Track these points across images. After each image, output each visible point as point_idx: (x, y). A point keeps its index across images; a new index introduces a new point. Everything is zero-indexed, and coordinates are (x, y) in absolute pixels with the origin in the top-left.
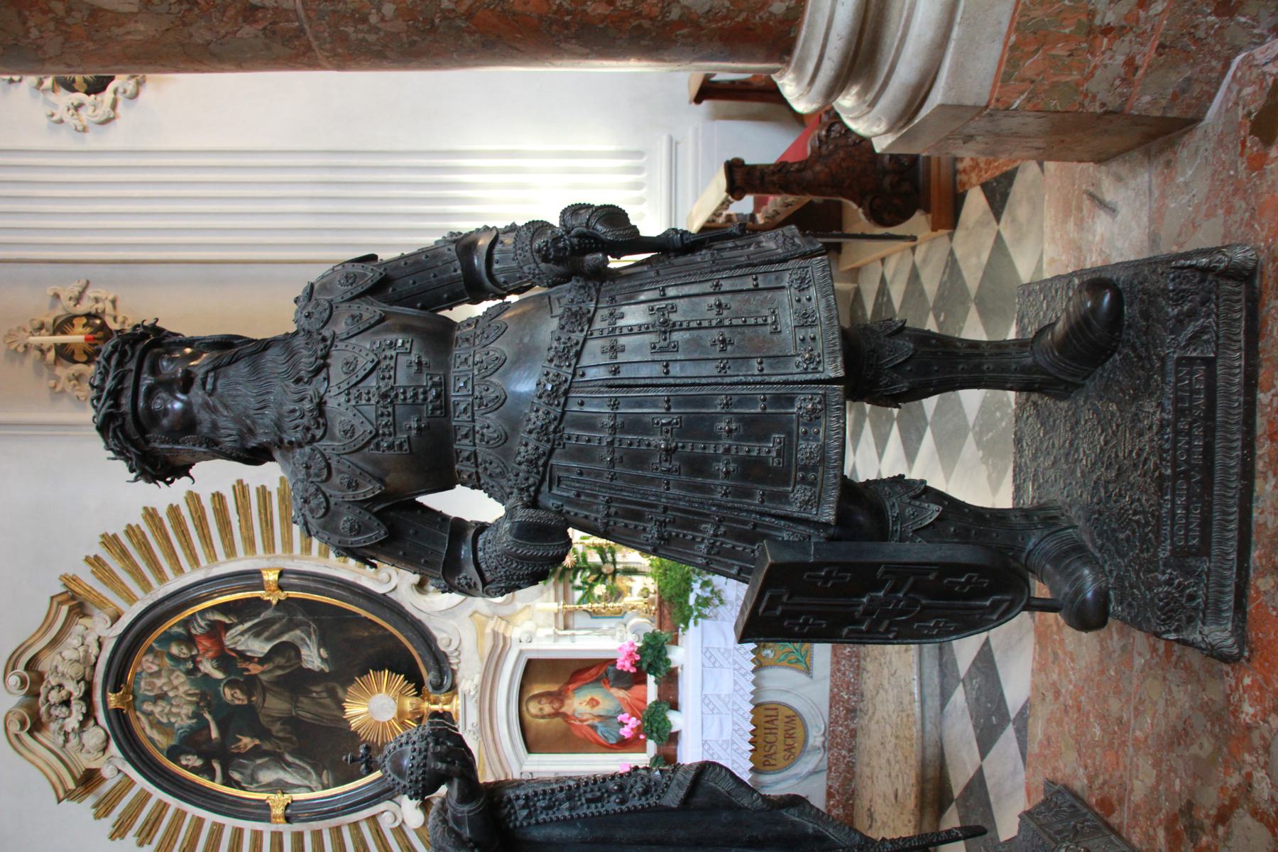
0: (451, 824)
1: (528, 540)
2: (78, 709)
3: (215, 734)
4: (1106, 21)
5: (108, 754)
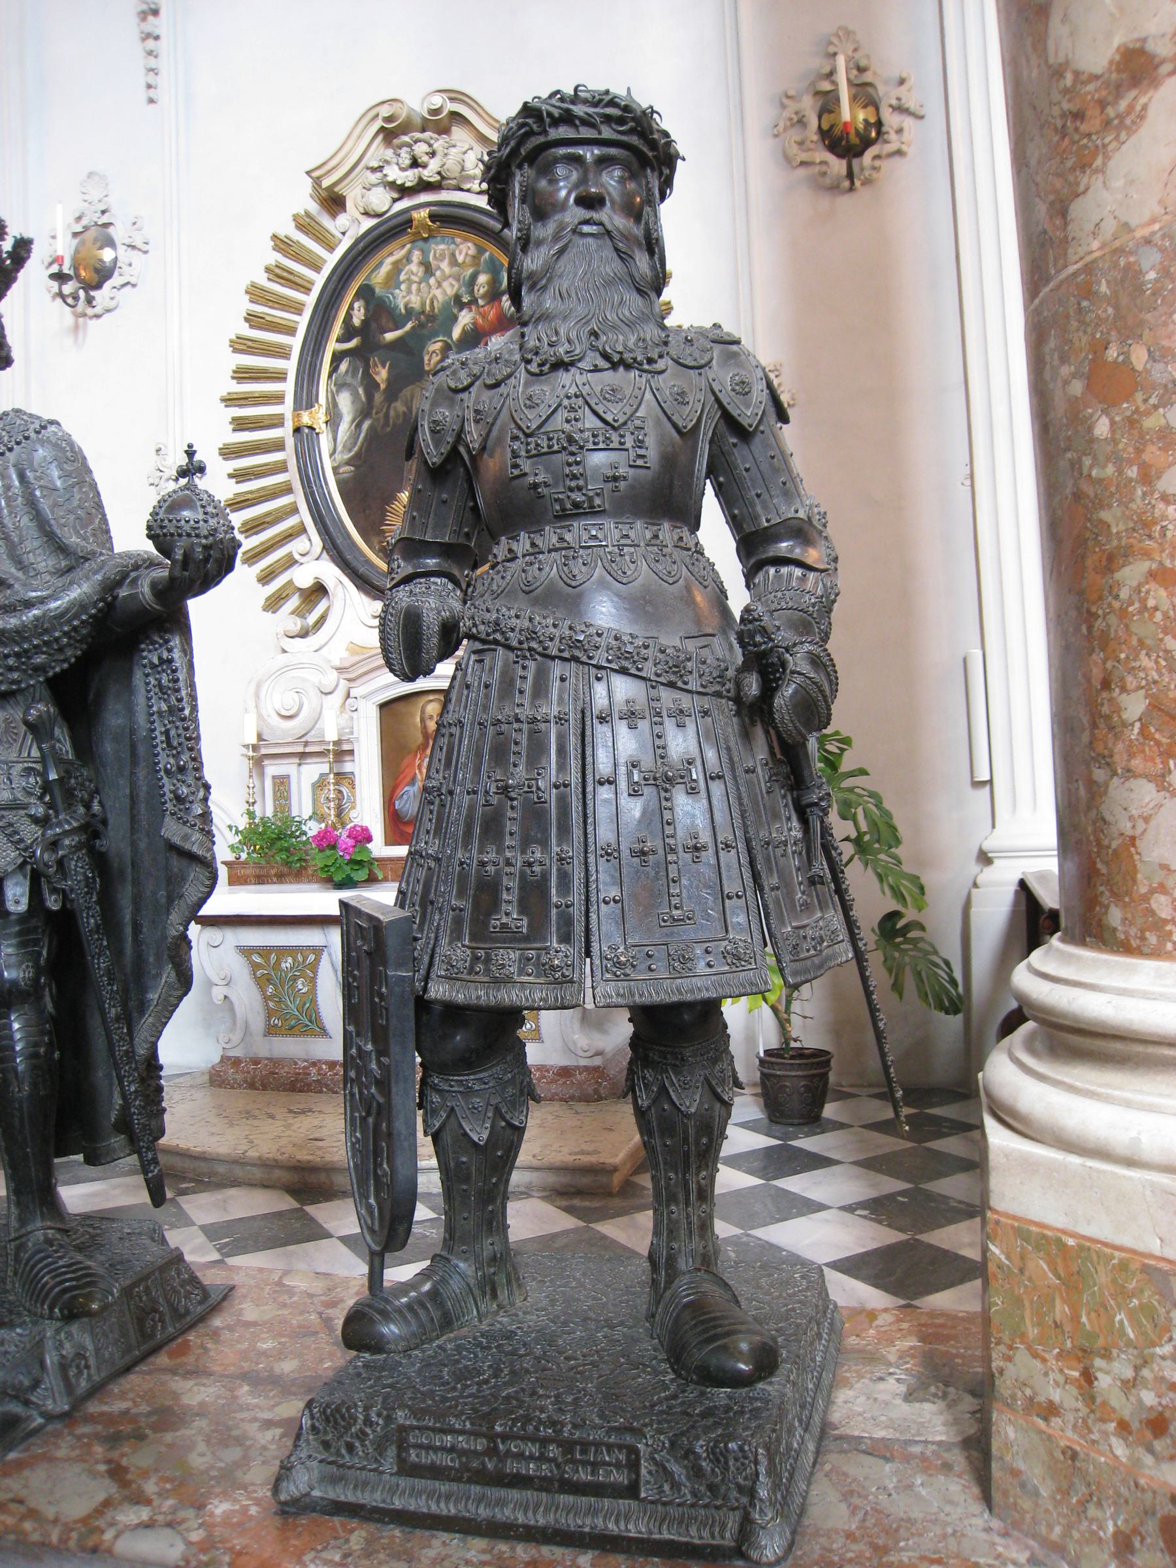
0: (133, 574)
1: (405, 626)
2: (408, 178)
3: (390, 336)
4: (1099, 1375)
5: (362, 218)
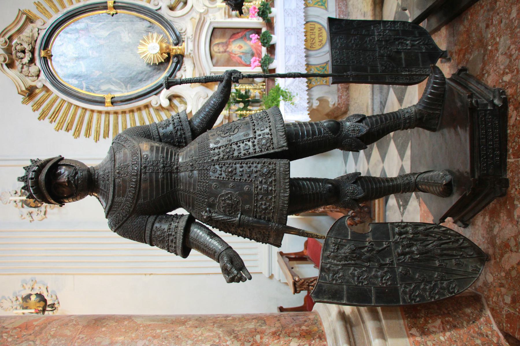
5: (40, 78)
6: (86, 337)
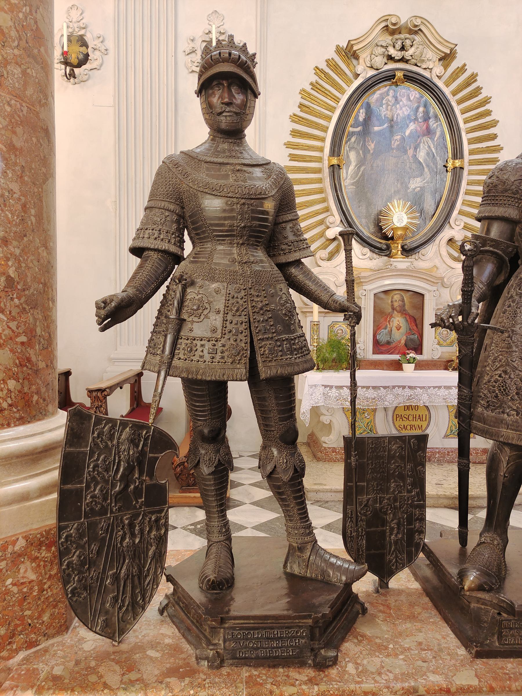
3: (376, 129)
6: (24, 115)
